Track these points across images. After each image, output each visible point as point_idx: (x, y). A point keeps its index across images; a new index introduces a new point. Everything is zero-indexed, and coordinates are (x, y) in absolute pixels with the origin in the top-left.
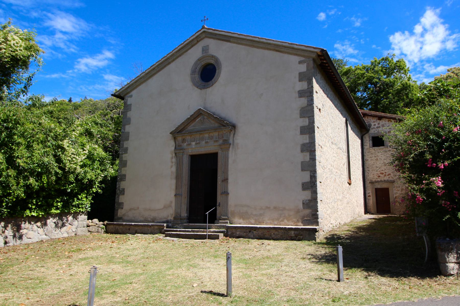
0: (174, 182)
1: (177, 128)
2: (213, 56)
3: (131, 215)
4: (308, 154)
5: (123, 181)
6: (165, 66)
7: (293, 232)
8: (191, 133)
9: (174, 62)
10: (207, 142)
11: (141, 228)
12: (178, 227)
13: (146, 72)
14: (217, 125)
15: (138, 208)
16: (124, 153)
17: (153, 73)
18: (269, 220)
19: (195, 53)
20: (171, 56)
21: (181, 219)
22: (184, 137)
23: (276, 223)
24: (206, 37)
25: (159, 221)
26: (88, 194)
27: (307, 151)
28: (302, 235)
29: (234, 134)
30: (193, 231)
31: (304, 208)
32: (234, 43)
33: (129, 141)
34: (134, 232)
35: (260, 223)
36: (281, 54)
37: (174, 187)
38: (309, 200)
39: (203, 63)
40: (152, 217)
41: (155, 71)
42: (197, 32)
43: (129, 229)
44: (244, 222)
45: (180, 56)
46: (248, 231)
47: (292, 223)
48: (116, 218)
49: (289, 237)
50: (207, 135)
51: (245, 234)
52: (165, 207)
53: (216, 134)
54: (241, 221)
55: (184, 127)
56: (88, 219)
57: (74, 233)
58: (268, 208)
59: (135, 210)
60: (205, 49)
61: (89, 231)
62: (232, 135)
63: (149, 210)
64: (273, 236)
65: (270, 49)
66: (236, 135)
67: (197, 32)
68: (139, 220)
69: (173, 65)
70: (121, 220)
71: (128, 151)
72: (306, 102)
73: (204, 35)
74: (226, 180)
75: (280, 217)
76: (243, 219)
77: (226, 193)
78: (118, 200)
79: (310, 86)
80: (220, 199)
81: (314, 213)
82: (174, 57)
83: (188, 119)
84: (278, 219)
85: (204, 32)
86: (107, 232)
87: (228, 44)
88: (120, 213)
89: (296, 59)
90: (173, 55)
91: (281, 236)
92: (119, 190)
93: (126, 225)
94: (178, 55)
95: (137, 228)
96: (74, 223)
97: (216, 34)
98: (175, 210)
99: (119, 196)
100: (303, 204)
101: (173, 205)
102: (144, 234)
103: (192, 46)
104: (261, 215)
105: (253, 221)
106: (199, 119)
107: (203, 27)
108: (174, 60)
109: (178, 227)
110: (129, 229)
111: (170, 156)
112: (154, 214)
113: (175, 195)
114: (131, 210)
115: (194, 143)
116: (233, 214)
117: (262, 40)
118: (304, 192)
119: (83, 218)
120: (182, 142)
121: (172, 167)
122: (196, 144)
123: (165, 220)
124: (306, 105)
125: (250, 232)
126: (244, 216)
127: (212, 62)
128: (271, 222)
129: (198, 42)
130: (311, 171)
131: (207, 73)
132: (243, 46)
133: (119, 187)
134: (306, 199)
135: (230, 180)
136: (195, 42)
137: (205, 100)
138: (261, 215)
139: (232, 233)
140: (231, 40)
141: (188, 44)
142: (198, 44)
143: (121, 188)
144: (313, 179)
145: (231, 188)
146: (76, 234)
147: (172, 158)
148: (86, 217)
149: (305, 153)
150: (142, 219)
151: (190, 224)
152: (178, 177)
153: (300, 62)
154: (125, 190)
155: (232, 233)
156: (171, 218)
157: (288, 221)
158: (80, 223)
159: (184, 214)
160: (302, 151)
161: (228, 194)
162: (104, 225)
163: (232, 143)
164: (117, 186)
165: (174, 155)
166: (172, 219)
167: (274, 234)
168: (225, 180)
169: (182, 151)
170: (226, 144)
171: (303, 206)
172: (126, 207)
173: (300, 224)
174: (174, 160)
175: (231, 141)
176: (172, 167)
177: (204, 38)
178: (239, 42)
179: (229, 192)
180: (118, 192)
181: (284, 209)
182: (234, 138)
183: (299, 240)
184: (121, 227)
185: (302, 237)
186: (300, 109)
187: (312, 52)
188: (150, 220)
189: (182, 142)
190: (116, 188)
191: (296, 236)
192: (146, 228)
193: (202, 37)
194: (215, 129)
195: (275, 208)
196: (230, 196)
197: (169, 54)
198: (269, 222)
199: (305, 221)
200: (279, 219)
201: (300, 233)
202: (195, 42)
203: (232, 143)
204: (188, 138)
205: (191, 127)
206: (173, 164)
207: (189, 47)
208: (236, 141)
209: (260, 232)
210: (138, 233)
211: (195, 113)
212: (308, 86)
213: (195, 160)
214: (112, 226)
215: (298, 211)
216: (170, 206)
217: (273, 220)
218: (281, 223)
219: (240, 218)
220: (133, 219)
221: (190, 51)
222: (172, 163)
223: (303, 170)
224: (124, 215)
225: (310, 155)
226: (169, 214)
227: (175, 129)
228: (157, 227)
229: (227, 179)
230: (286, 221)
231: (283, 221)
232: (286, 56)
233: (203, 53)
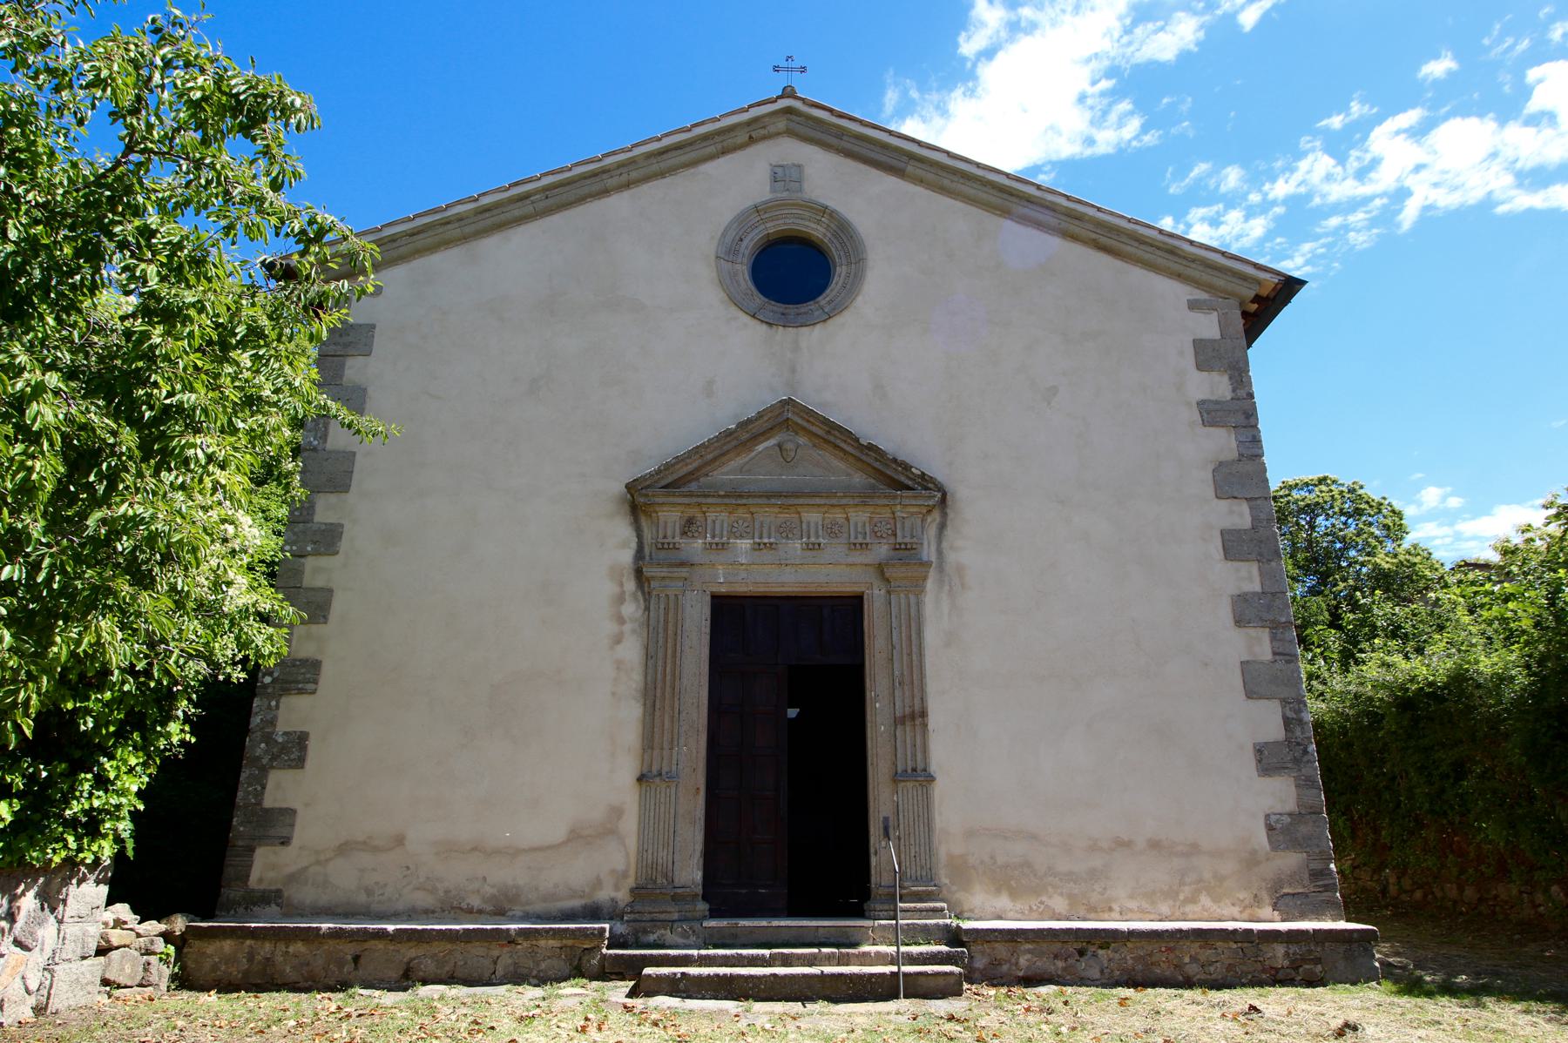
0: (632, 713)
1: (668, 466)
2: (824, 210)
3: (345, 879)
4: (1265, 635)
5: (301, 692)
6: (581, 200)
7: (1280, 950)
8: (736, 496)
9: (626, 194)
10: (814, 547)
11: (440, 948)
12: (669, 937)
13: (486, 201)
14: (858, 479)
15: (400, 841)
16: (316, 553)
17: (517, 213)
18: (1131, 897)
19: (738, 186)
20: (621, 165)
21: (675, 898)
22: (691, 512)
23: (1165, 909)
24: (790, 133)
25: (539, 907)
26: (143, 747)
27: (1262, 622)
28: (1318, 961)
29: (942, 526)
30: (787, 961)
31: (1275, 846)
32: (920, 181)
33: (351, 497)
34: (394, 974)
35: (1093, 911)
36: (1118, 263)
37: (631, 735)
38: (1290, 814)
39: (772, 228)
40: (489, 890)
41: (529, 209)
42: (759, 104)
43: (356, 959)
44: (1019, 906)
45: (661, 174)
46: (1071, 948)
47: (1235, 911)
48: (230, 893)
49: (1264, 971)
50: (813, 517)
51: (1060, 964)
52: (578, 837)
53: (860, 517)
54: (1003, 902)
55: (698, 469)
56: (110, 901)
57: (32, 1001)
58: (1123, 844)
59: (376, 850)
60: (782, 176)
61: (105, 982)
62: (932, 531)
63: (475, 849)
64: (1192, 970)
65: (1074, 238)
66: (949, 532)
67: (759, 104)
68: (400, 906)
69: (619, 204)
70: (274, 908)
71: (344, 545)
72: (1234, 444)
73: (781, 124)
74: (916, 717)
75: (1182, 883)
76: (1014, 894)
77: (919, 776)
78: (259, 795)
79: (1242, 393)
80: (882, 798)
81: (1316, 865)
82: (634, 175)
83: (728, 434)
84: (1171, 894)
85: (788, 111)
86: (184, 981)
87: (891, 181)
88: (266, 867)
89: (1179, 293)
90: (632, 162)
91: (1230, 967)
92: (268, 739)
93: (336, 934)
94: (655, 168)
95: (410, 952)
96: (40, 933)
97: (841, 133)
98: (642, 851)
99: (264, 771)
100: (1270, 828)
101: (630, 824)
102: (469, 982)
103: (725, 152)
104: (1093, 875)
105: (1059, 904)
106: (772, 442)
107: (788, 93)
108: (628, 185)
109: (669, 937)
110: (356, 959)
111: (609, 588)
112: (504, 875)
113: (641, 779)
114: (344, 849)
115: (744, 544)
116: (962, 871)
117: (1050, 197)
118: (1268, 780)
119: (88, 894)
120: (684, 533)
121: (618, 640)
122: (758, 547)
123: (576, 903)
124: (1235, 455)
125: (1081, 953)
126: (1013, 880)
127: (817, 230)
128: (1145, 905)
129: (752, 140)
130: (1285, 702)
131: (792, 271)
132: (959, 205)
133: (272, 722)
134: (1278, 809)
135: (935, 720)
136: (742, 137)
137: (793, 371)
138: (1093, 875)
139: (995, 963)
140: (910, 169)
141: (706, 137)
142: (751, 150)
143: (281, 727)
144: (1298, 733)
145: (942, 753)
146: (39, 1010)
147: (620, 599)
148: (104, 890)
149: (1252, 632)
150: (423, 900)
151: (744, 923)
152: (656, 695)
153: (1193, 305)
154: (312, 745)
155: (995, 963)
156: (615, 892)
157: (1216, 899)
158: (71, 929)
159: (691, 873)
160: (1240, 622)
161: (931, 779)
162: (167, 937)
163: (933, 558)
164: (256, 721)
165: (630, 585)
166: (623, 896)
167: (1194, 959)
168: (913, 717)
169: (684, 572)
170: (907, 564)
171: (1269, 837)
172: (309, 833)
173: (1267, 911)
174: (631, 609)
175: (929, 552)
176: (618, 640)
177: (778, 134)
178: (946, 182)
179: (934, 768)
180: (256, 747)
181: (1194, 850)
182: (945, 545)
183: (1311, 984)
184: (298, 947)
185: (1319, 968)
186: (1211, 467)
187: (1244, 277)
188: (476, 902)
189: (684, 533)
190: (244, 729)
191: (1295, 966)
192: (477, 949)
193: (772, 129)
194: (864, 498)
195: (1155, 845)
196: (941, 789)
197: (614, 153)
198: (1133, 905)
199: (1287, 899)
200: (1177, 894)
201: (1310, 951)
202: (742, 137)
203: (933, 558)
204: (718, 517)
205: (727, 473)
206: (627, 627)
207: (711, 149)
208: (951, 557)
209: (1129, 956)
210: (425, 982)
211: (760, 415)
212: (1234, 391)
213: (733, 616)
214: (228, 945)
215: (1251, 861)
216: (608, 830)
217: (1151, 896)
218: (1189, 908)
219: (998, 891)
220: (362, 898)
221: (708, 168)
222: (621, 620)
223: (1250, 694)
224: (292, 878)
225: (1273, 638)
226: (608, 870)
227: (658, 472)
228: (552, 943)
229: (923, 714)
230: (1205, 900)
231: (1193, 900)
232: (1137, 274)
233: (773, 190)
